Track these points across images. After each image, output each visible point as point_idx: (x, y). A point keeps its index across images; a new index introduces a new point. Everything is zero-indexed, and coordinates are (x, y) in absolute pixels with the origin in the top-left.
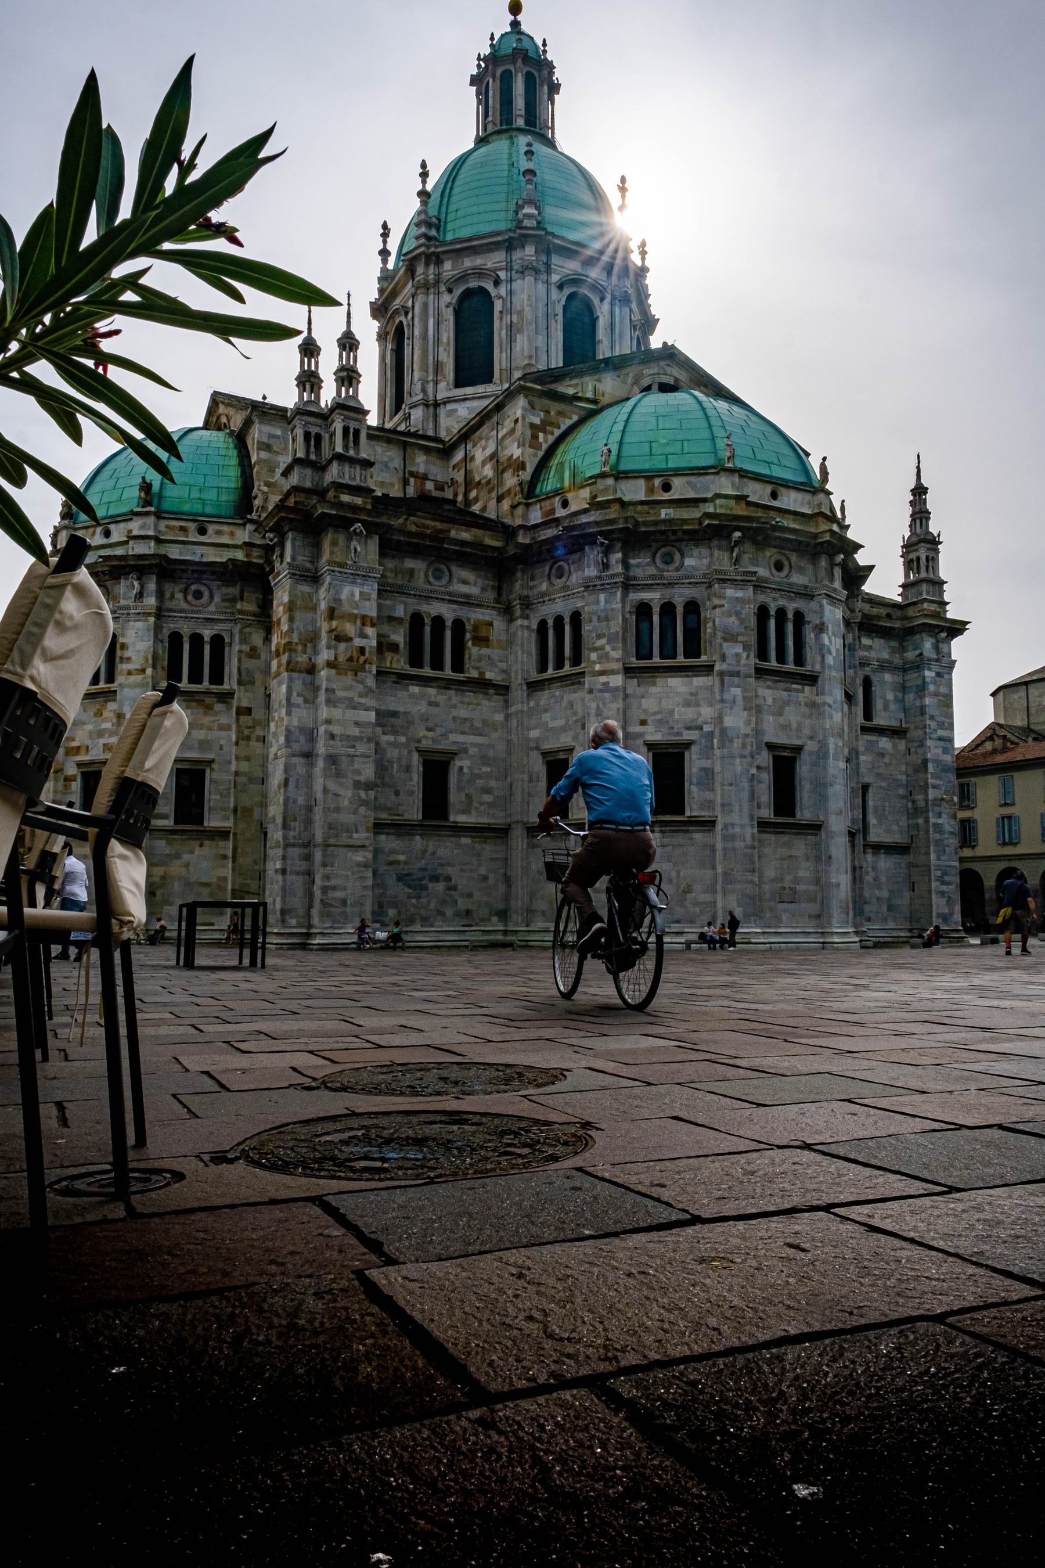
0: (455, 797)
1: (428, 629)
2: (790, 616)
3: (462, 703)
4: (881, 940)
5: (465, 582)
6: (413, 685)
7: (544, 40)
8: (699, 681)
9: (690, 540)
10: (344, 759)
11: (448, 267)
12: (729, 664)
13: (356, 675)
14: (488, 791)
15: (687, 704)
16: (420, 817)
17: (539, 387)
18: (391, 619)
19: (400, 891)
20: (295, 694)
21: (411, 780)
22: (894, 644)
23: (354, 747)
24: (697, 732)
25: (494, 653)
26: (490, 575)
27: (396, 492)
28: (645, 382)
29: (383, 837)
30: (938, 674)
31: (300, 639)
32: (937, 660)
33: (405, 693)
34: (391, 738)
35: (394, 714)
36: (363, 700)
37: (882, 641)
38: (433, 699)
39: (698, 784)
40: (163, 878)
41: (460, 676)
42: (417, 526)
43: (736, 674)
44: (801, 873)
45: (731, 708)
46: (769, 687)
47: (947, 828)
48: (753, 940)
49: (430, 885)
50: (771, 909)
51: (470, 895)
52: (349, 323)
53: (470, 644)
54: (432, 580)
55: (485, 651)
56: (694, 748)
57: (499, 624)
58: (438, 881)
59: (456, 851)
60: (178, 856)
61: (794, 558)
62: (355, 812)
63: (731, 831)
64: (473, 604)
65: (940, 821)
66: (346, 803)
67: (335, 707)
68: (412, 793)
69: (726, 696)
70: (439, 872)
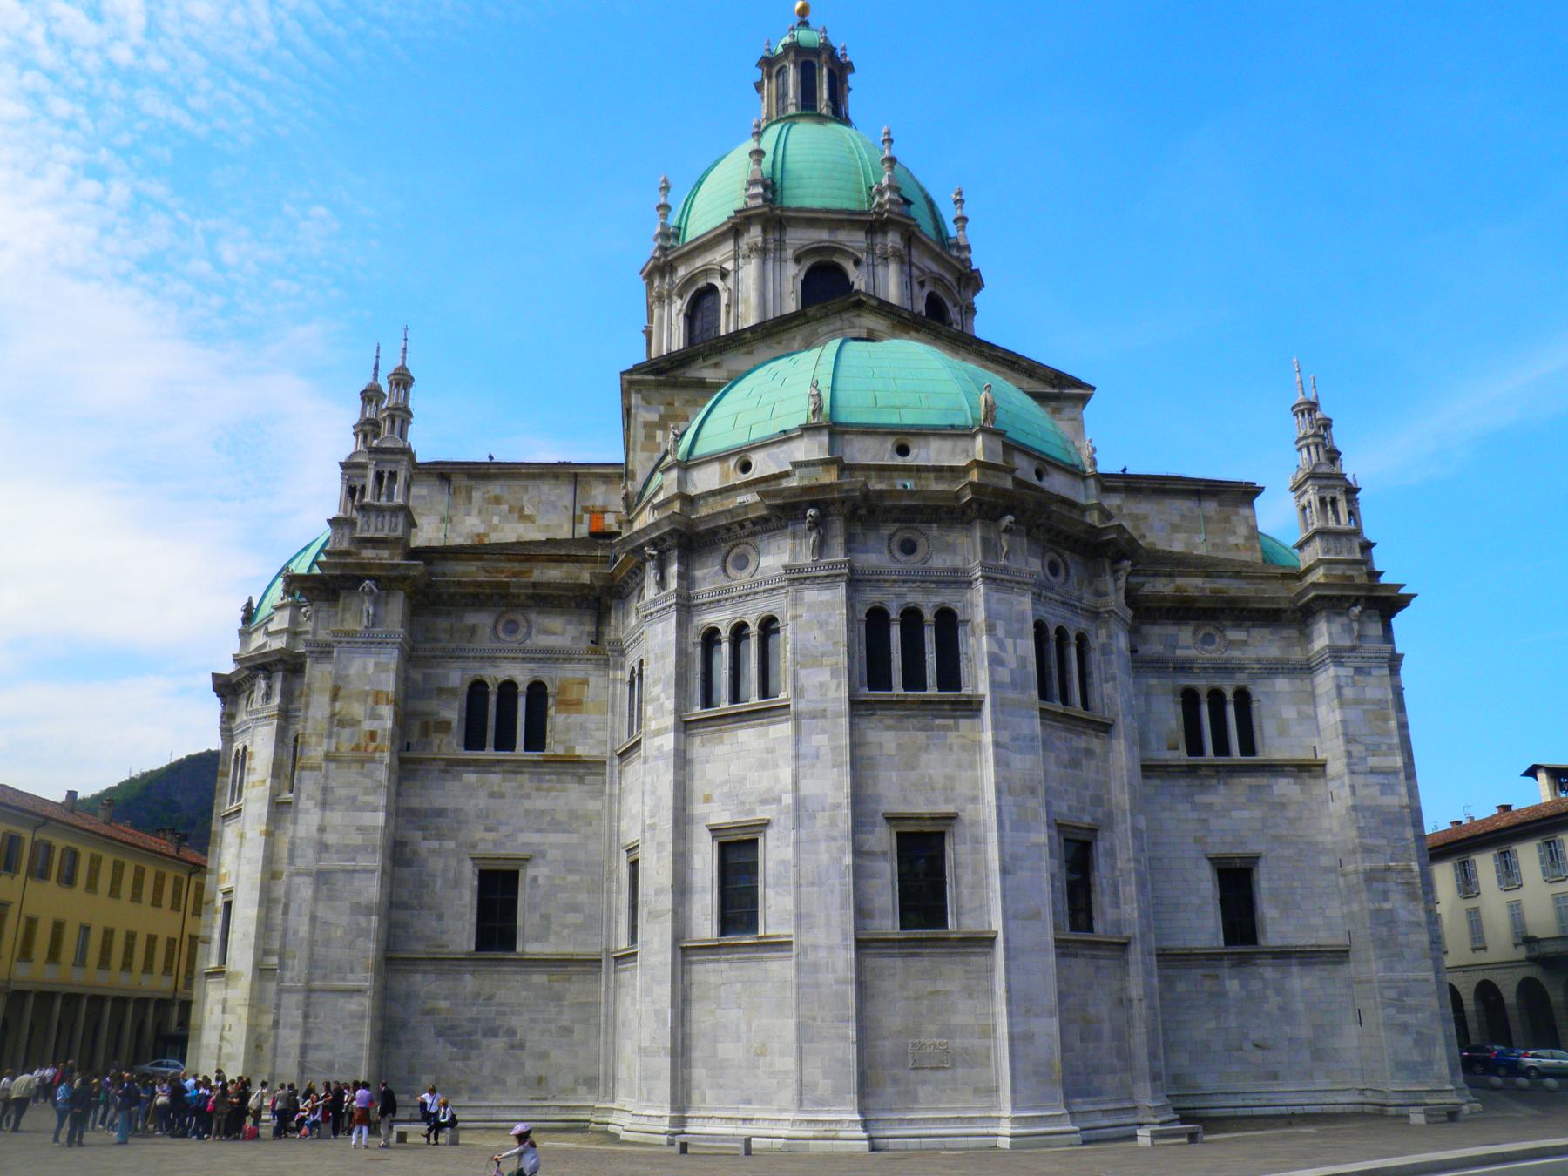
0: (526, 919)
1: (493, 699)
2: (929, 616)
3: (537, 790)
4: (1298, 1110)
5: (546, 632)
6: (468, 772)
7: (824, 28)
9: (766, 531)
10: (341, 876)
11: (682, 272)
12: (808, 701)
13: (362, 767)
14: (575, 908)
15: (763, 765)
16: (473, 947)
17: (653, 378)
18: (441, 691)
20: (303, 796)
21: (460, 899)
22: (1293, 633)
23: (354, 859)
24: (774, 806)
25: (591, 719)
26: (587, 619)
27: (564, 533)
29: (418, 977)
30: (1358, 671)
31: (315, 729)
32: (1353, 649)
33: (457, 784)
34: (435, 844)
35: (440, 813)
36: (370, 799)
37: (1266, 631)
38: (496, 789)
39: (776, 885)
41: (534, 755)
42: (486, 571)
43: (823, 714)
44: (957, 1020)
45: (813, 766)
46: (888, 728)
47: (1403, 915)
48: (842, 1134)
49: (485, 1042)
50: (895, 1081)
51: (543, 1056)
52: (404, 358)
53: (551, 711)
54: (502, 635)
55: (574, 718)
56: (771, 833)
57: (595, 680)
58: (496, 1035)
59: (524, 993)
61: (935, 530)
62: (351, 946)
63: (811, 957)
64: (557, 659)
65: (1387, 906)
66: (340, 932)
67: (332, 809)
69: (803, 750)
70: (498, 1023)
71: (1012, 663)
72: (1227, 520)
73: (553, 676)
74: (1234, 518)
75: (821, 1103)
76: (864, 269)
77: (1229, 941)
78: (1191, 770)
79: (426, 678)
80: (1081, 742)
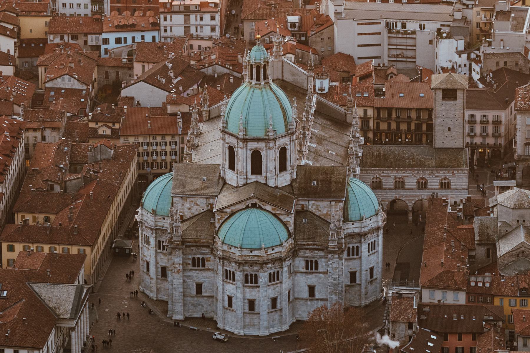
0: (203, 290)
5: (204, 250)
8: (235, 286)
14: (210, 289)
19: (192, 307)
25: (212, 263)
28: (247, 204)
35: (190, 276)
40: (160, 287)
41: (203, 268)
44: (255, 321)
47: (334, 298)
55: (209, 263)
57: (212, 258)
60: (162, 283)
68: (194, 290)
71: (264, 281)
72: (337, 206)
73: (206, 257)
74: (338, 205)
75: (239, 329)
76: (264, 152)
77: (309, 296)
78: (306, 273)
79: (186, 257)
80: (276, 286)
